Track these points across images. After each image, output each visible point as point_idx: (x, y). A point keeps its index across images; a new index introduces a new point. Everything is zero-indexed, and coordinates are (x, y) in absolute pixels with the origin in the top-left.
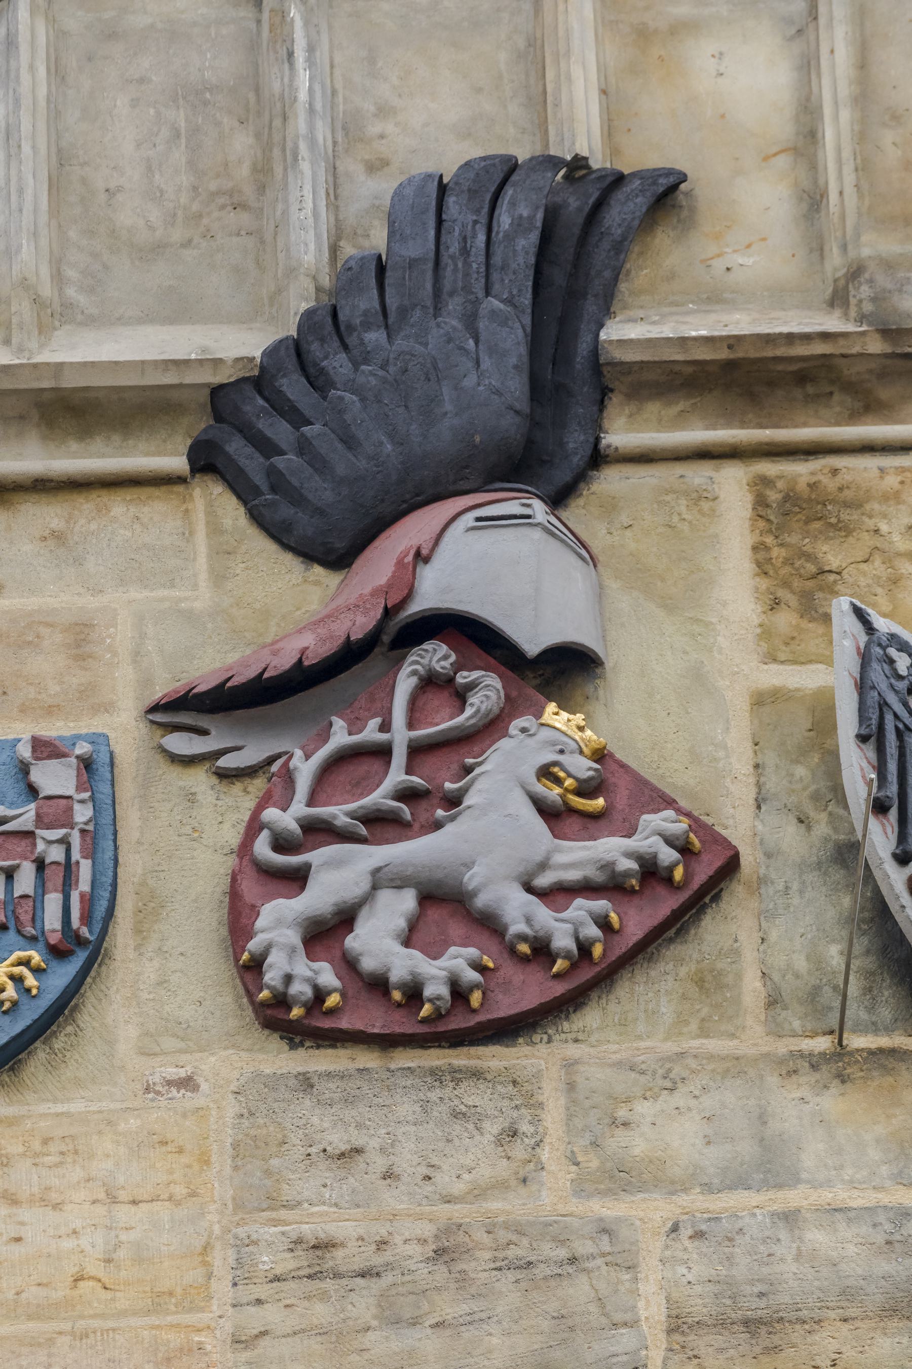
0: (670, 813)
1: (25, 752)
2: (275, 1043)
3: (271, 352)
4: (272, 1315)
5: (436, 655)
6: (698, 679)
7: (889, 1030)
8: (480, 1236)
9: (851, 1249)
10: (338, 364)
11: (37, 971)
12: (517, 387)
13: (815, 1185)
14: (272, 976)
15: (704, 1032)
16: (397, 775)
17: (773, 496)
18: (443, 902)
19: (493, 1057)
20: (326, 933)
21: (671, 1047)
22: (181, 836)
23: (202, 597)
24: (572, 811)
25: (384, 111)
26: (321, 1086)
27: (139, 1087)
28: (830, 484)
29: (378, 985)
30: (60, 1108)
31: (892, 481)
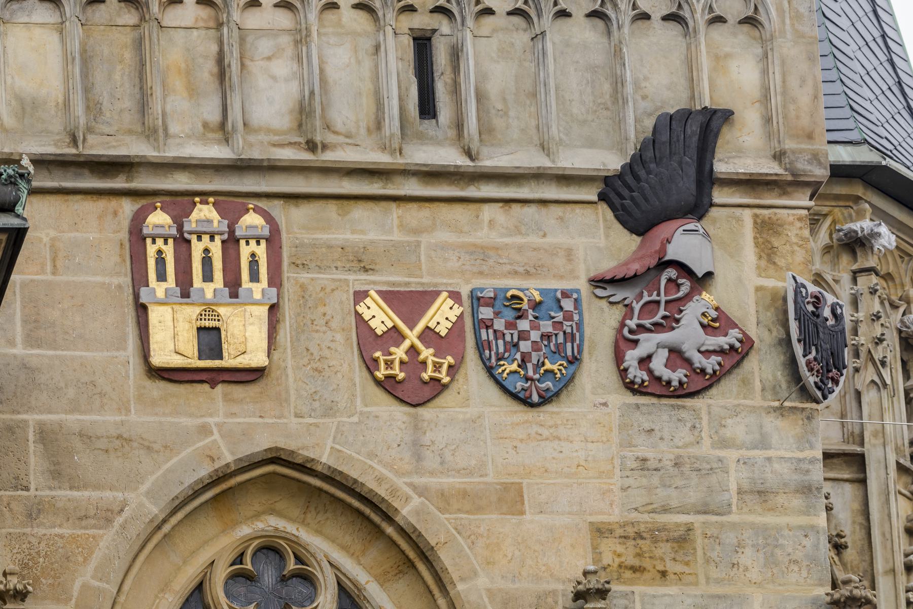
0: (737, 330)
1: (559, 295)
2: (629, 393)
3: (623, 167)
4: (630, 481)
5: (672, 273)
6: (740, 280)
7: (794, 401)
8: (686, 459)
9: (786, 471)
10: (642, 173)
11: (565, 368)
12: (693, 187)
13: (776, 449)
14: (631, 376)
15: (745, 398)
16: (662, 312)
17: (759, 221)
18: (676, 354)
19: (688, 402)
20: (645, 361)
21: (736, 402)
22: (600, 322)
23: (602, 242)
24: (709, 325)
25: (646, 79)
26: (642, 408)
27: (592, 405)
28: (775, 218)
29: (659, 379)
30: (570, 410)
31: (791, 218)
